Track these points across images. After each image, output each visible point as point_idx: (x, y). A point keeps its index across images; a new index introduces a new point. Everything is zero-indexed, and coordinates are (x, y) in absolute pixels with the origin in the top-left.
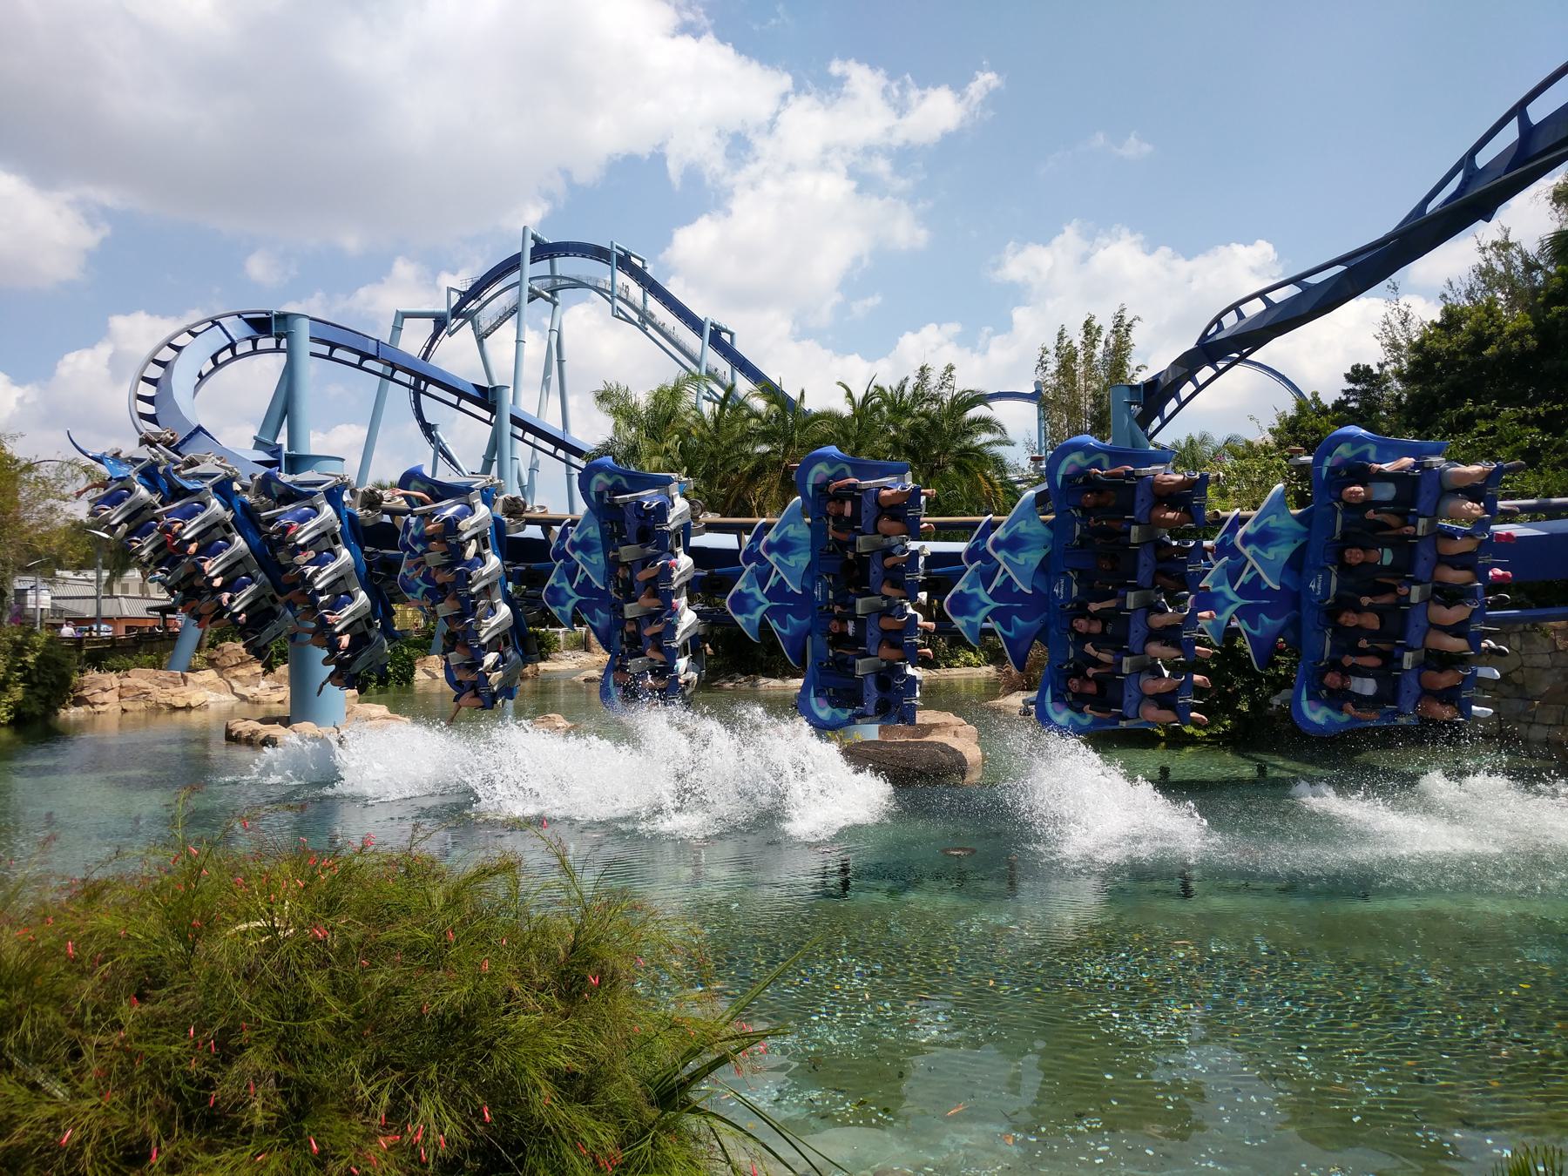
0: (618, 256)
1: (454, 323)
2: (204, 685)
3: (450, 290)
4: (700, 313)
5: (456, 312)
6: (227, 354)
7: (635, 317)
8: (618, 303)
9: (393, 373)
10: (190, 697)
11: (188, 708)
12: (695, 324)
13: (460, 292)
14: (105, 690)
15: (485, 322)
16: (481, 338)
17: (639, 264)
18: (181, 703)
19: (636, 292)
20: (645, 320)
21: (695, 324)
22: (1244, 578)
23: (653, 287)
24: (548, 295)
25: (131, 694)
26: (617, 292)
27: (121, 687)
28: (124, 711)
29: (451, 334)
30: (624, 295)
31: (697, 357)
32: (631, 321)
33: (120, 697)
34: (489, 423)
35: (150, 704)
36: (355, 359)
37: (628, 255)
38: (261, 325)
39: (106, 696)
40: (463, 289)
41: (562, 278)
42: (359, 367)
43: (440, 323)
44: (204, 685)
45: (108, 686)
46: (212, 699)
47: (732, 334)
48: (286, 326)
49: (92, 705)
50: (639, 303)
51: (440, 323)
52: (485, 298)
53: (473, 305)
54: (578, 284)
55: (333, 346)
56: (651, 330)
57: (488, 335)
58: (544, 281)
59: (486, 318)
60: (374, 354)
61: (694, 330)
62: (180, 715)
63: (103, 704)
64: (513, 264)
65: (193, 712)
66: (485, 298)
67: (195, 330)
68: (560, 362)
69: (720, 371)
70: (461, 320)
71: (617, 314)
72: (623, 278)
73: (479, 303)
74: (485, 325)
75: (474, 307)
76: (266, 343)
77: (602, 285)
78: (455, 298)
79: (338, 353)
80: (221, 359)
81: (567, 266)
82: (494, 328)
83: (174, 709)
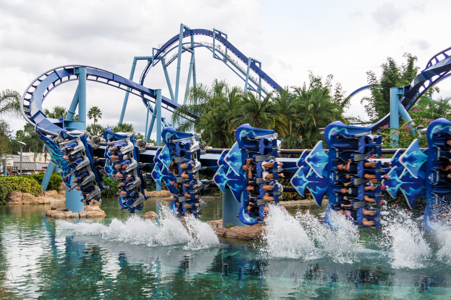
0: (216, 34)
1: (155, 61)
2: (51, 196)
3: (154, 49)
4: (247, 55)
5: (156, 58)
6: (59, 81)
7: (222, 57)
8: (216, 52)
9: (119, 85)
10: (44, 200)
11: (44, 204)
12: (245, 59)
13: (157, 50)
14: (18, 197)
15: (167, 60)
16: (165, 67)
17: (224, 37)
18: (41, 202)
19: (223, 48)
20: (226, 59)
21: (245, 59)
22: (403, 173)
23: (229, 46)
24: (190, 50)
25: (26, 198)
26: (216, 48)
27: (22, 196)
28: (23, 204)
29: (153, 66)
30: (218, 49)
31: (246, 73)
32: (219, 59)
33: (22, 199)
34: (155, 103)
35: (31, 202)
36: (106, 81)
37: (220, 33)
38: (69, 71)
39: (18, 199)
40: (159, 49)
41: (195, 43)
42: (107, 83)
43: (150, 61)
44: (51, 196)
45: (19, 195)
46: (53, 201)
47: (260, 63)
48: (78, 71)
49: (13, 201)
50: (224, 52)
51: (150, 61)
52: (166, 52)
53: (162, 54)
54: (201, 45)
55: (98, 77)
56: (228, 63)
57: (167, 66)
58: (188, 44)
59: (168, 58)
60: (112, 79)
61: (244, 62)
62: (41, 206)
63: (17, 201)
64: (176, 38)
65: (45, 206)
66: (166, 52)
67: (48, 74)
68: (194, 75)
69: (255, 78)
70: (157, 60)
71: (215, 56)
72: (217, 42)
73: (164, 54)
74: (166, 62)
75: (162, 55)
76: (73, 77)
77: (210, 45)
78: (156, 52)
79: (99, 79)
80: (56, 84)
81: (198, 38)
82: (170, 63)
83: (40, 204)
